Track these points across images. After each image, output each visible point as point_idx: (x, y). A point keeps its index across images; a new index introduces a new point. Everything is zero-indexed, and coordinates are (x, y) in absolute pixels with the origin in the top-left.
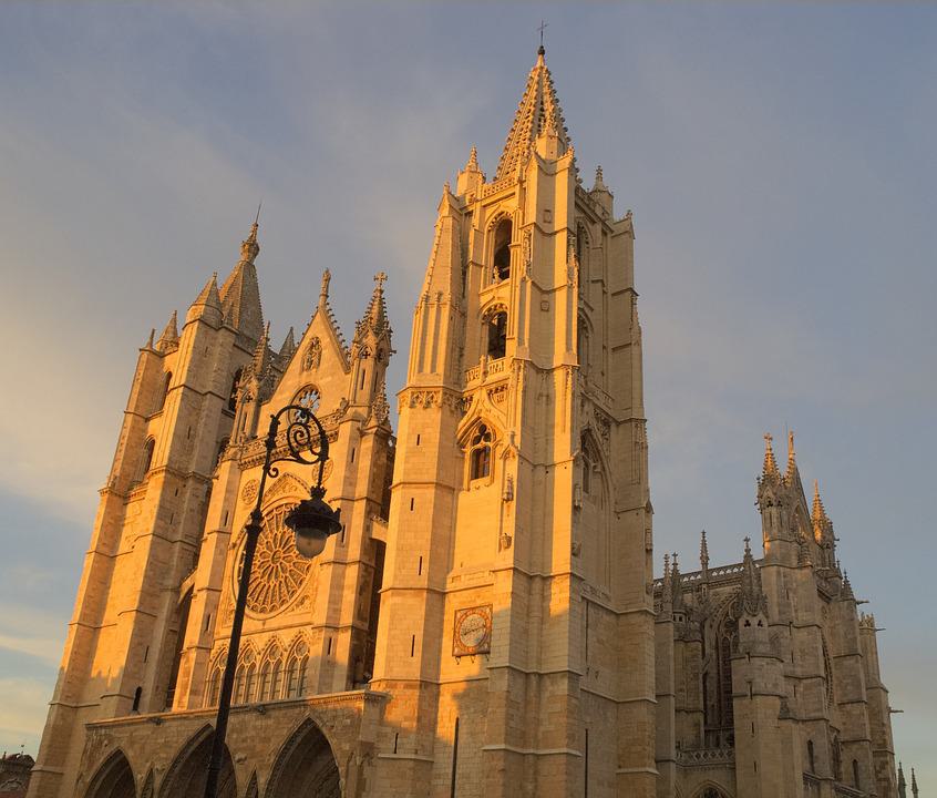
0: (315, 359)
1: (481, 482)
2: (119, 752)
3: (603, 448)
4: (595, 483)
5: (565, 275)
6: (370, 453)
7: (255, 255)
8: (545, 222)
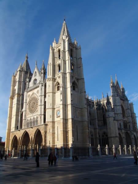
1: (59, 91)
2: (15, 136)
3: (77, 84)
4: (76, 89)
5: (68, 58)
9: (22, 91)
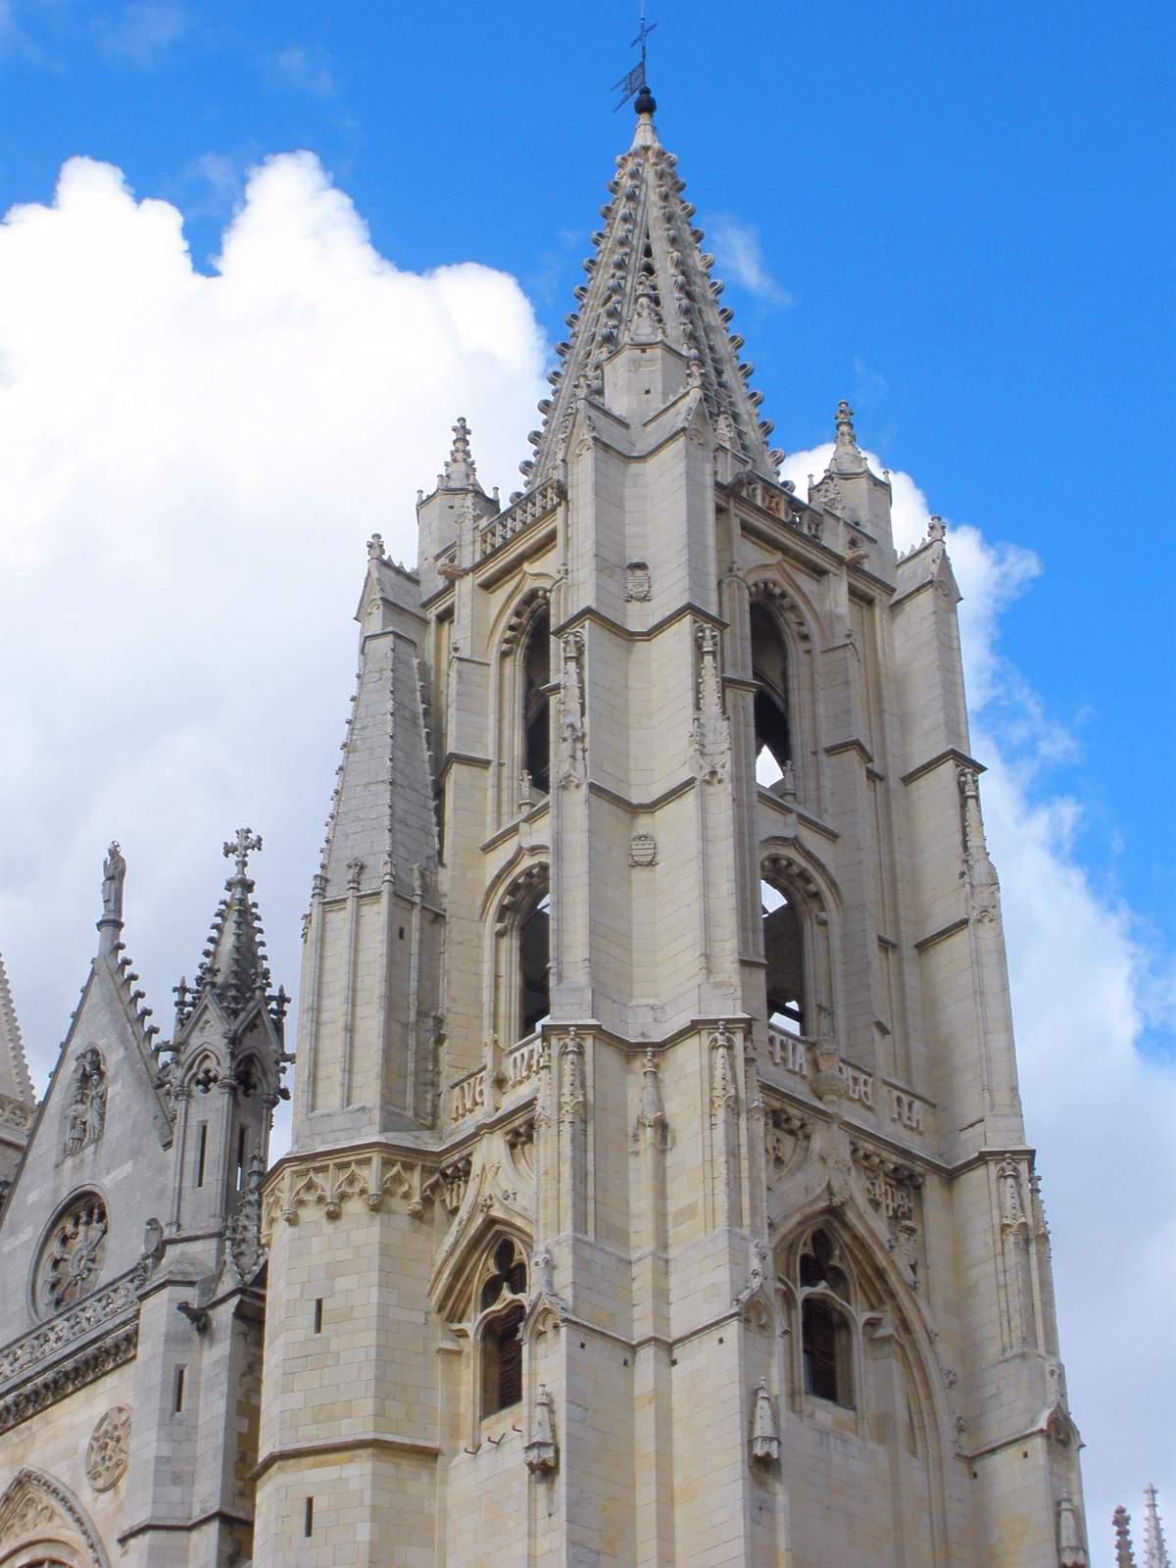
0: (92, 1118)
3: (898, 1263)
6: (224, 1376)
8: (630, 599)
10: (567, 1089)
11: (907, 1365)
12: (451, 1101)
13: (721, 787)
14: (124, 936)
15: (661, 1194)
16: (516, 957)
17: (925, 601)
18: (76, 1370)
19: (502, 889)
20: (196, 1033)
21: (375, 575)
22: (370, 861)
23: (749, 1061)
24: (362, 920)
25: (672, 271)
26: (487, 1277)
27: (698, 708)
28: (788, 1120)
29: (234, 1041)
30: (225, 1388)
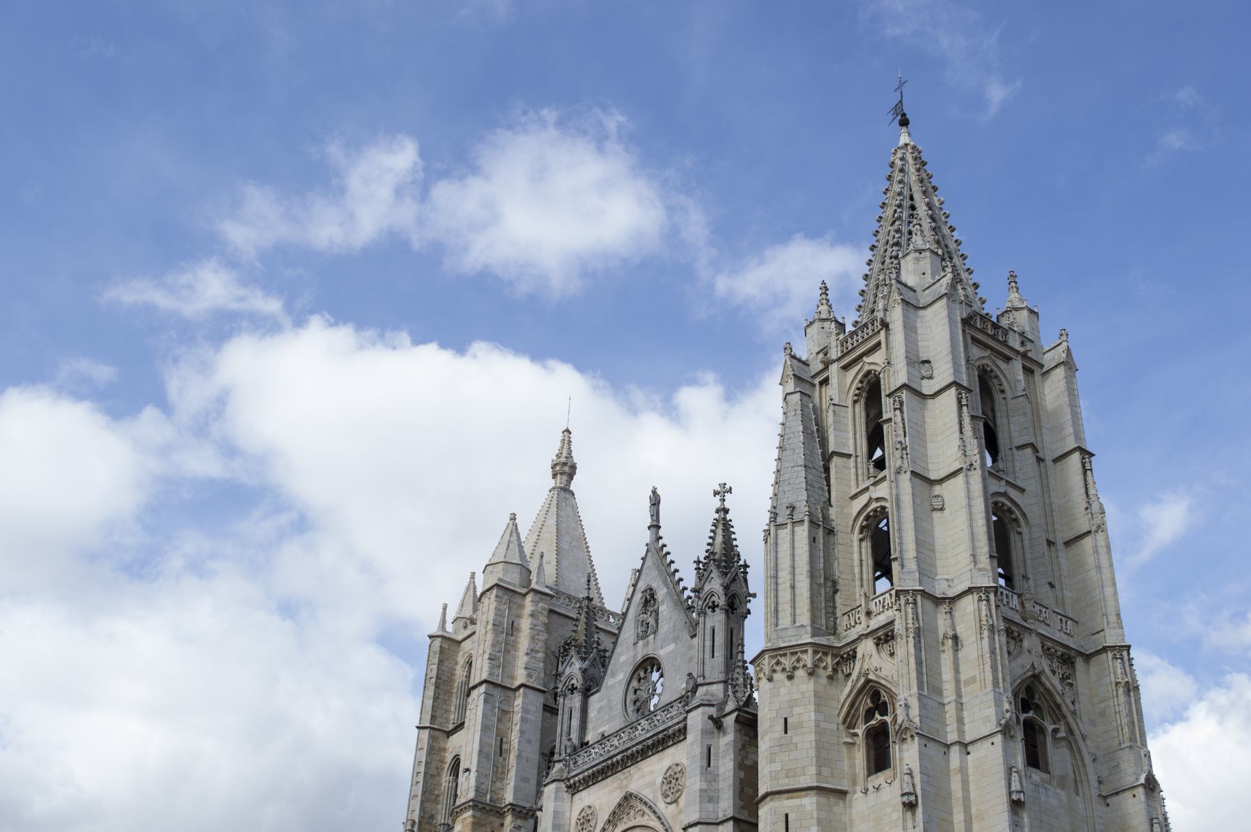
0: (651, 621)
1: (880, 778)
4: (1057, 756)
6: (731, 750)
7: (571, 476)
8: (923, 378)
9: (521, 779)
10: (910, 621)
11: (1071, 748)
12: (843, 622)
13: (975, 472)
14: (661, 533)
15: (957, 671)
16: (870, 551)
17: (1060, 373)
18: (653, 745)
19: (861, 519)
20: (707, 584)
21: (789, 363)
22: (797, 505)
23: (997, 607)
24: (795, 534)
25: (925, 208)
26: (867, 708)
27: (961, 433)
28: (1012, 632)
29: (726, 588)
30: (732, 756)
